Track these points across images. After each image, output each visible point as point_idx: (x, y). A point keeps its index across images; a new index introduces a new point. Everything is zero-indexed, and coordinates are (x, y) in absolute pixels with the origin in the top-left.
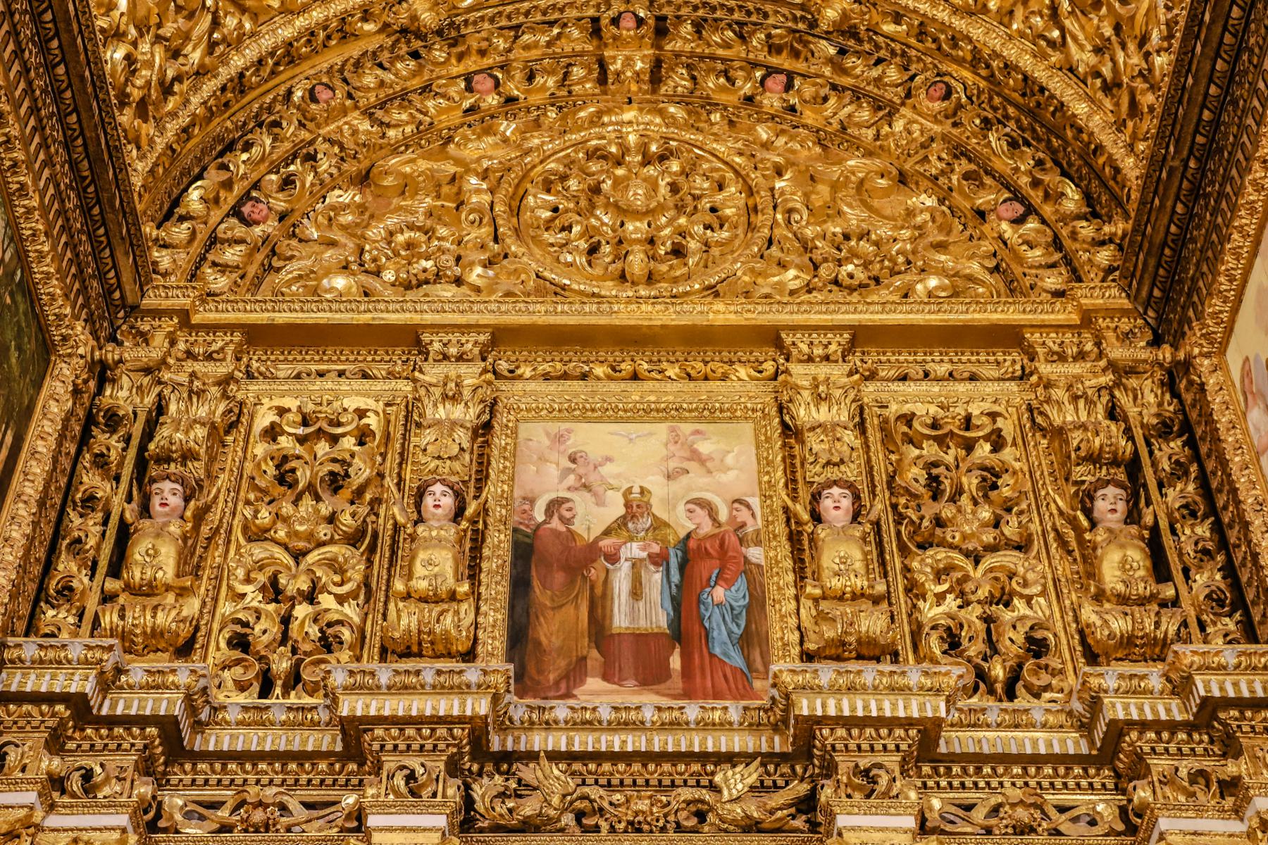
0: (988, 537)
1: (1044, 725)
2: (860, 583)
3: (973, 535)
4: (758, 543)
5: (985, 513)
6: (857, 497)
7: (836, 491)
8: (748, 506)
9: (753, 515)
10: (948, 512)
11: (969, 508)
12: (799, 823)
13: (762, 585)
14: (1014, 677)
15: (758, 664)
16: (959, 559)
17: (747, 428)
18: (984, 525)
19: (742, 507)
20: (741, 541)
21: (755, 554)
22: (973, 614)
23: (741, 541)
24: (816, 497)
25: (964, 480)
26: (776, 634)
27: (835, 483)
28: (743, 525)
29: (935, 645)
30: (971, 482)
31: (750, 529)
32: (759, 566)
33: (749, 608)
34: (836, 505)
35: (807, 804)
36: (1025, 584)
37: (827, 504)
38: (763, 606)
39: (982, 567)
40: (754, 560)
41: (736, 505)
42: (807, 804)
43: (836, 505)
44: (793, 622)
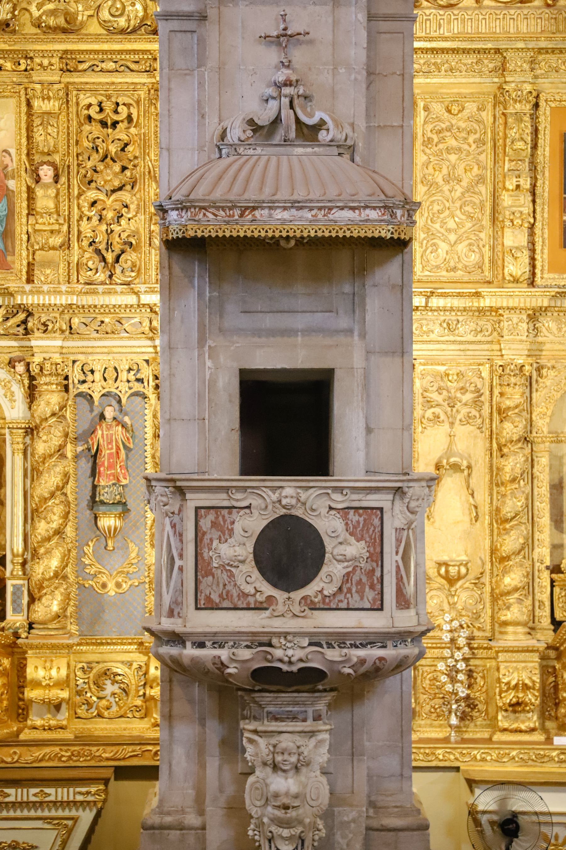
0: (117, 183)
1: (121, 292)
2: (52, 221)
3: (110, 181)
4: (13, 178)
5: (117, 168)
6: (56, 169)
7: (45, 167)
8: (10, 154)
9: (12, 160)
10: (101, 167)
11: (111, 162)
12: (21, 330)
13: (14, 203)
14: (117, 260)
15: (10, 249)
16: (102, 197)
17: (12, 102)
18: (116, 174)
19: (7, 155)
20: (6, 176)
21: (12, 184)
22: (104, 227)
23: (6, 176)
24: (37, 169)
25: (110, 147)
26: (18, 230)
27: (45, 163)
28: (7, 166)
29: (85, 243)
30: (113, 149)
31: (10, 169)
32: (13, 192)
33: (7, 216)
34: (46, 173)
35: (25, 322)
36: (128, 212)
37: (41, 173)
38: (13, 215)
39: (112, 198)
40: (11, 188)
41: (4, 154)
42: (25, 322)
43: (46, 173)
44: (25, 229)
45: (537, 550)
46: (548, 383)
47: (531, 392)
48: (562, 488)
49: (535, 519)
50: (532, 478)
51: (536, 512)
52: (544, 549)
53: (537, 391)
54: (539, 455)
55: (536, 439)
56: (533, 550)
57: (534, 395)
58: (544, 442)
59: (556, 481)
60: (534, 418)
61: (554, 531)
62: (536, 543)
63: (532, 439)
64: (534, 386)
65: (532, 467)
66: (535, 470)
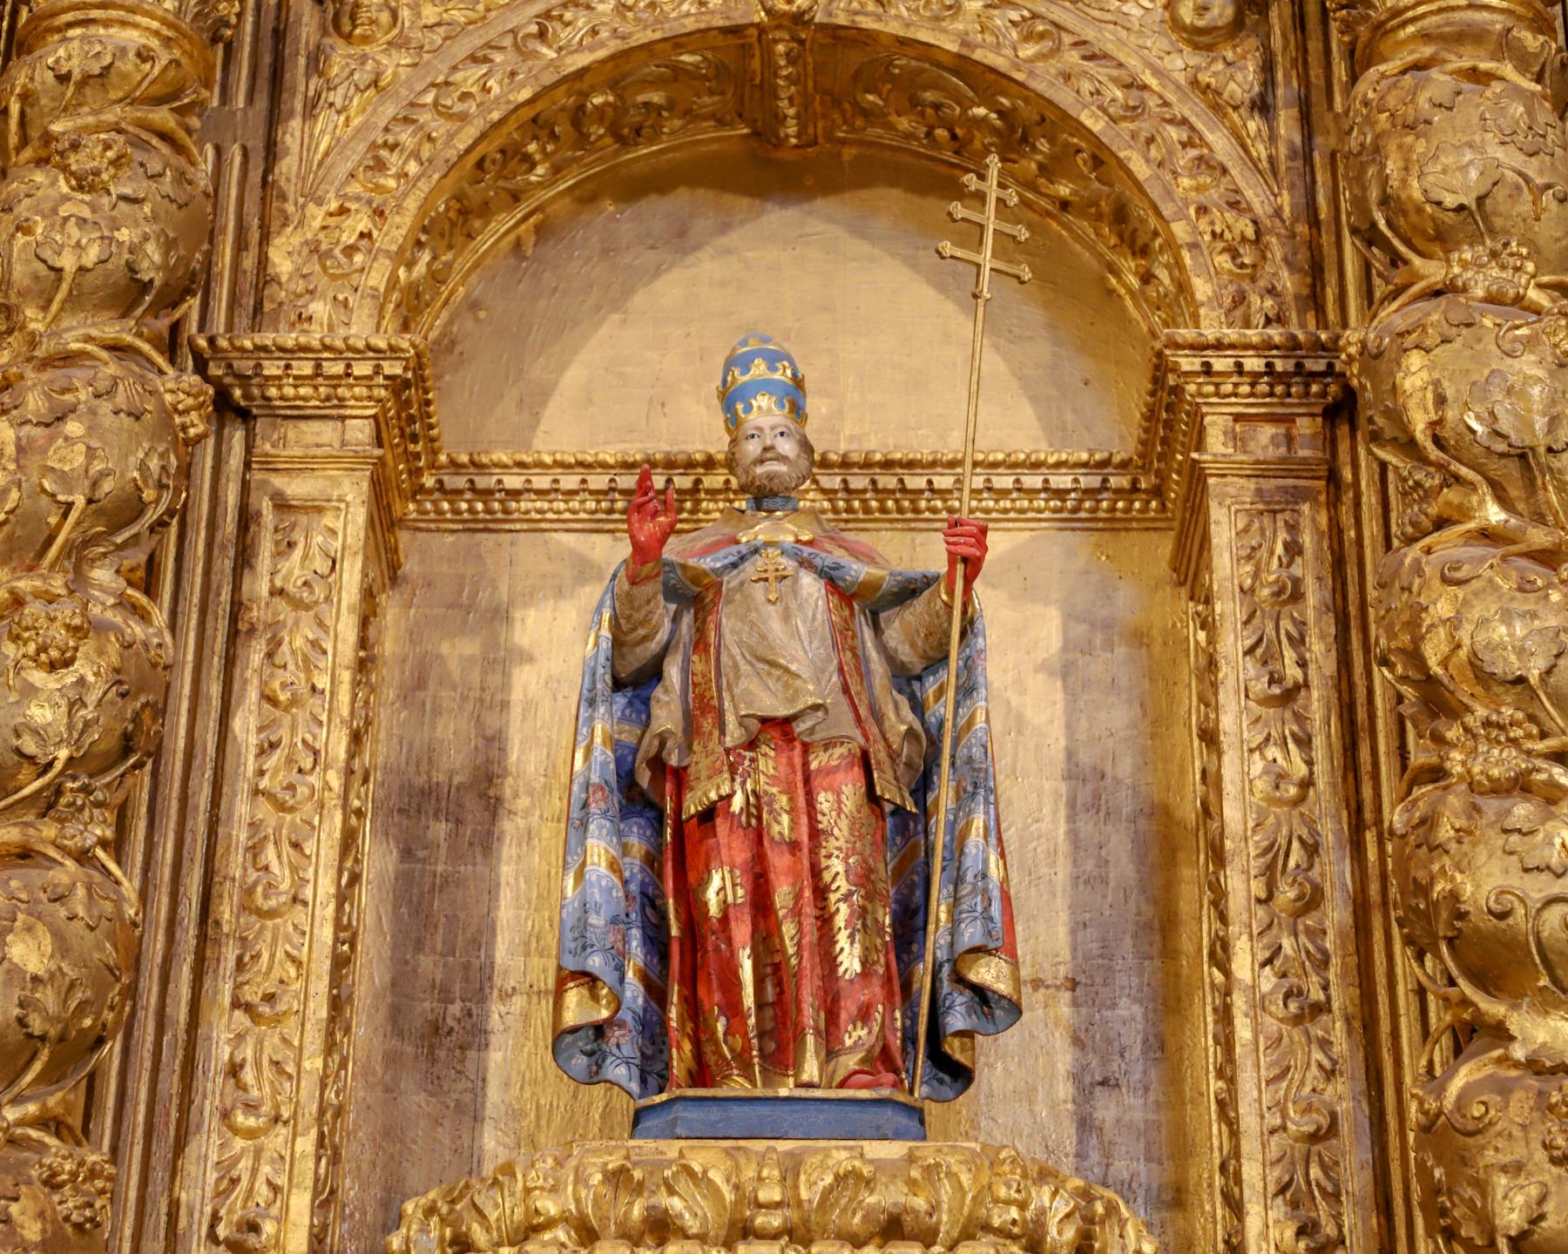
45: (207, 1148)
46: (394, 64)
47: (274, 118)
48: (493, 807)
49: (225, 911)
50: (233, 635)
51: (235, 865)
52: (277, 1140)
53: (311, 109)
54: (297, 488)
55: (272, 368)
56: (180, 1147)
57: (292, 133)
58: (333, 410)
59: (455, 761)
60: (282, 262)
61: (416, 1100)
62: (212, 1091)
63: (246, 366)
64: (301, 83)
65: (244, 559)
66: (259, 585)
